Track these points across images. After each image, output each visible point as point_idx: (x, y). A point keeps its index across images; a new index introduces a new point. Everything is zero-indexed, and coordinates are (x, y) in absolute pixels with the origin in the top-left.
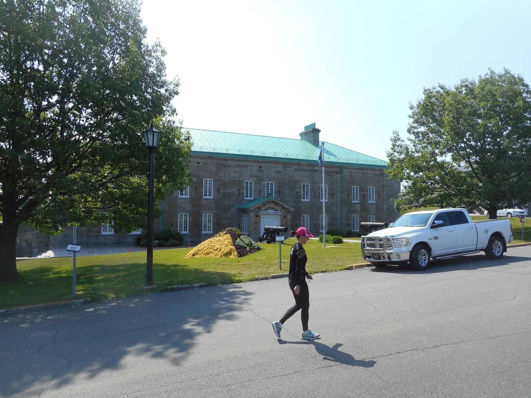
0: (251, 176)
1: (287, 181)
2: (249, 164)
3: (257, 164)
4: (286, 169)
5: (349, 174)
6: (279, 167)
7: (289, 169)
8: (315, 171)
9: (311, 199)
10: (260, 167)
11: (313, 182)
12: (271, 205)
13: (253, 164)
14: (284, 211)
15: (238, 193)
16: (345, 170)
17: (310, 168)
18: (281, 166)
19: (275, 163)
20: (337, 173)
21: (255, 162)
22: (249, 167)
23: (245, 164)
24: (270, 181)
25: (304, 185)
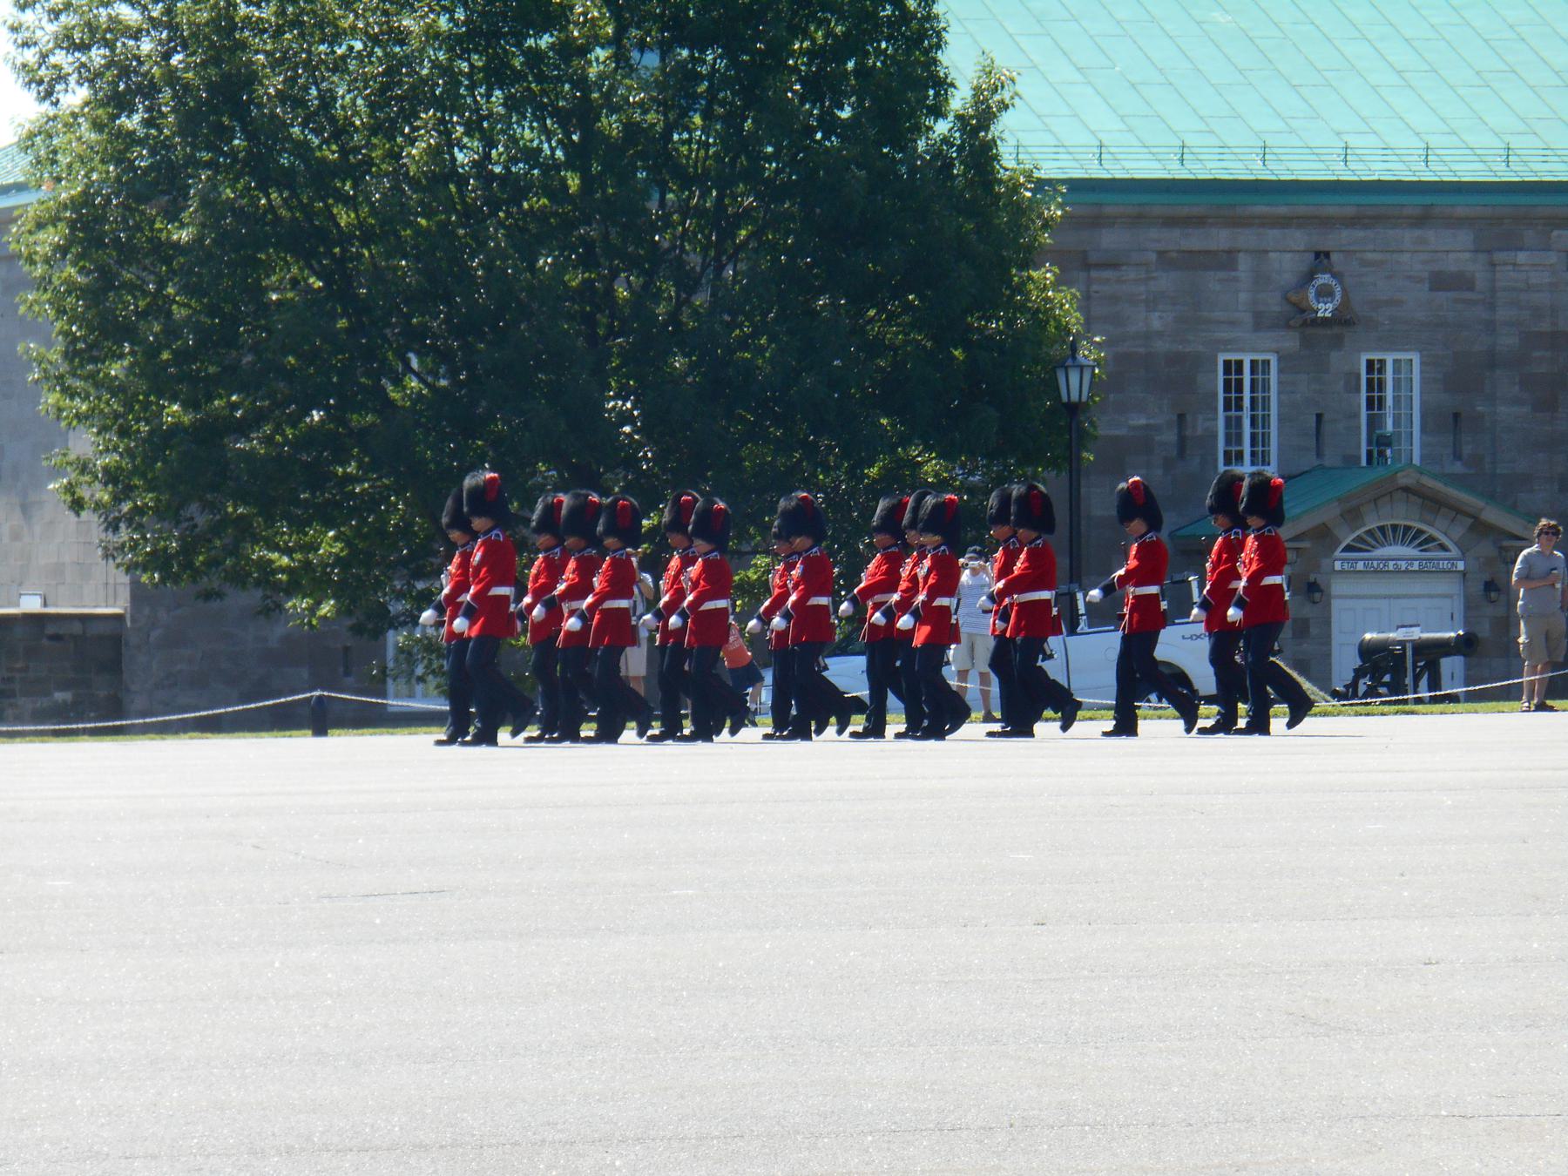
0: (1261, 322)
1: (1508, 341)
2: (1247, 238)
3: (1299, 239)
4: (1499, 256)
6: (1455, 250)
7: (1522, 257)
10: (1322, 256)
13: (1273, 234)
15: (1170, 437)
18: (1464, 238)
19: (1423, 219)
21: (1284, 222)
22: (1244, 263)
23: (1220, 239)
24: (1391, 344)
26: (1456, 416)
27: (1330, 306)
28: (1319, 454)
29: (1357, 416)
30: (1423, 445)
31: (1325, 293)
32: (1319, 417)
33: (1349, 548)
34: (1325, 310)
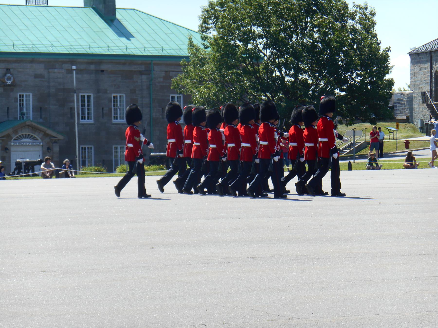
1: (53, 90)
4: (50, 70)
5: (163, 74)
6: (40, 69)
7: (56, 70)
8: (102, 71)
9: (96, 119)
11: (99, 91)
12: (27, 132)
14: (47, 140)
16: (156, 68)
17: (92, 67)
18: (42, 66)
19: (32, 61)
20: (141, 73)
25: (83, 97)
26: (41, 108)
27: (10, 82)
28: (8, 117)
29: (17, 108)
30: (33, 115)
31: (9, 79)
32: (8, 108)
33: (15, 140)
34: (9, 82)
